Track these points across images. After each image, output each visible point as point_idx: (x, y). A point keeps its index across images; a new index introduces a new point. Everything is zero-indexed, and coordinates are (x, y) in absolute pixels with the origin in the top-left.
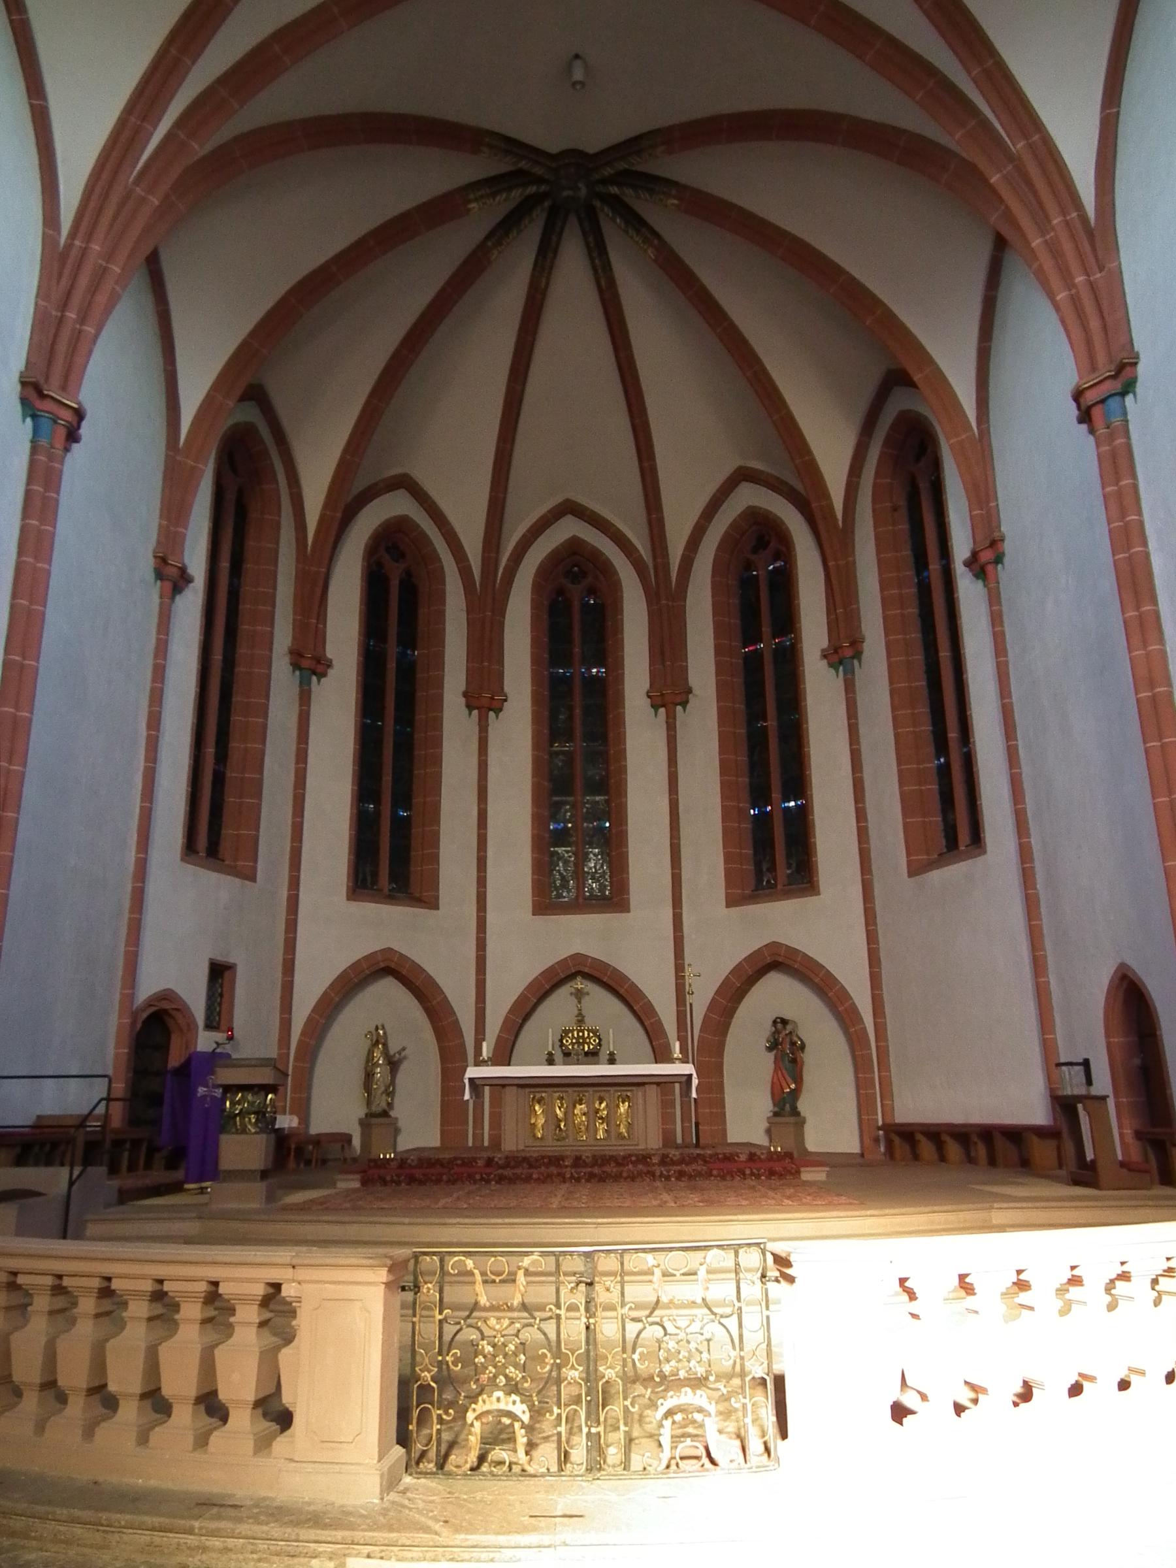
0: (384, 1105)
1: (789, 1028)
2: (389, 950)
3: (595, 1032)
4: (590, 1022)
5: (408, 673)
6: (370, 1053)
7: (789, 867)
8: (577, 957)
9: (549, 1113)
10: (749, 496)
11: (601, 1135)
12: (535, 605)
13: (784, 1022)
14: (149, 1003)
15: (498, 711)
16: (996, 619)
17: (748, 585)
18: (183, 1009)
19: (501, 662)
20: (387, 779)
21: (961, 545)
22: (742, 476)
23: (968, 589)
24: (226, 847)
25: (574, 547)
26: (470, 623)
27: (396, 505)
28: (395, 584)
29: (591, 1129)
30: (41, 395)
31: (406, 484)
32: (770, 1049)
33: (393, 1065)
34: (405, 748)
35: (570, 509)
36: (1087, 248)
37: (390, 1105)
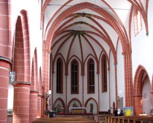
5: (60, 71)
10: (90, 57)
17: (90, 65)
21: (107, 68)
22: (90, 54)
23: (108, 71)
25: (75, 59)
27: (59, 56)
31: (60, 54)
34: (60, 79)
35: (74, 56)
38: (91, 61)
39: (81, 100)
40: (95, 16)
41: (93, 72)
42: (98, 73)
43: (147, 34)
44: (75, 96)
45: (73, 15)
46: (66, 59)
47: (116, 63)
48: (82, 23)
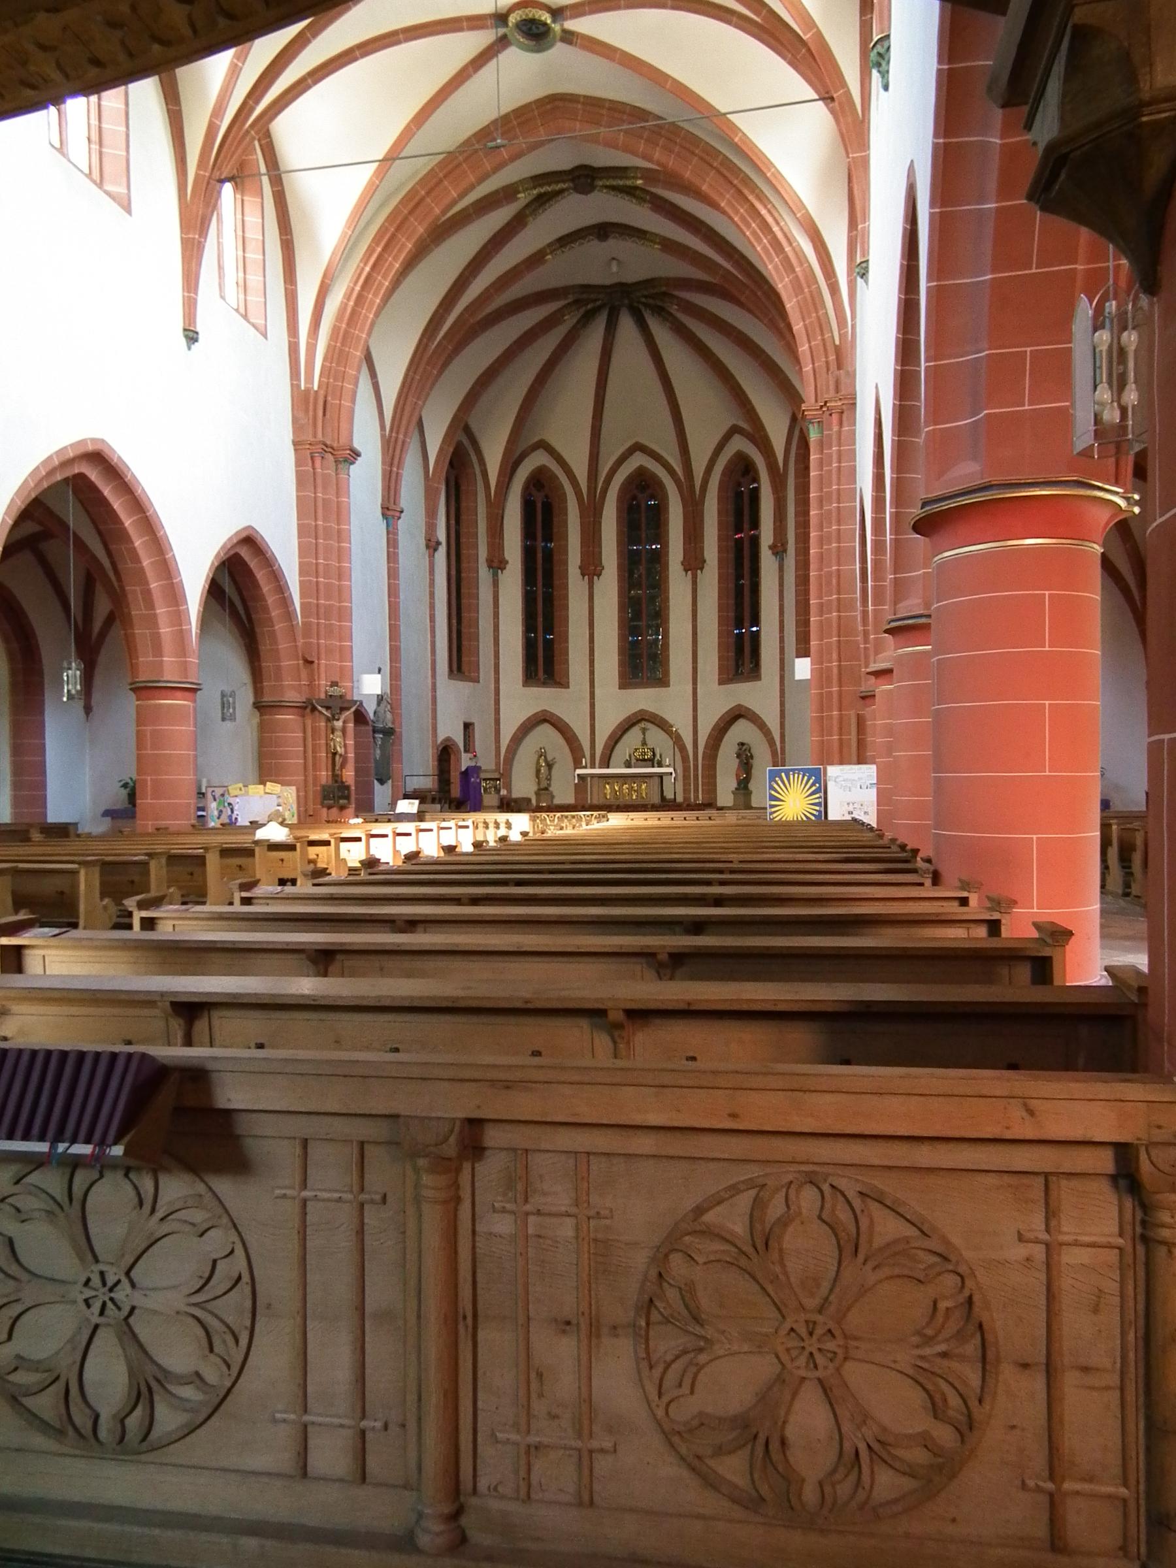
1: (744, 747)
4: (650, 744)
5: (549, 556)
6: (538, 760)
7: (751, 663)
9: (612, 788)
10: (739, 444)
11: (634, 797)
12: (619, 510)
13: (742, 744)
14: (441, 743)
15: (599, 575)
17: (739, 495)
18: (455, 744)
19: (600, 546)
20: (540, 619)
22: (734, 430)
24: (465, 667)
26: (582, 524)
28: (539, 505)
29: (630, 794)
30: (388, 509)
33: (550, 766)
34: (549, 600)
35: (638, 448)
37: (549, 785)
38: (743, 469)
41: (755, 542)
44: (643, 699)
45: (507, 194)
48: (603, 231)
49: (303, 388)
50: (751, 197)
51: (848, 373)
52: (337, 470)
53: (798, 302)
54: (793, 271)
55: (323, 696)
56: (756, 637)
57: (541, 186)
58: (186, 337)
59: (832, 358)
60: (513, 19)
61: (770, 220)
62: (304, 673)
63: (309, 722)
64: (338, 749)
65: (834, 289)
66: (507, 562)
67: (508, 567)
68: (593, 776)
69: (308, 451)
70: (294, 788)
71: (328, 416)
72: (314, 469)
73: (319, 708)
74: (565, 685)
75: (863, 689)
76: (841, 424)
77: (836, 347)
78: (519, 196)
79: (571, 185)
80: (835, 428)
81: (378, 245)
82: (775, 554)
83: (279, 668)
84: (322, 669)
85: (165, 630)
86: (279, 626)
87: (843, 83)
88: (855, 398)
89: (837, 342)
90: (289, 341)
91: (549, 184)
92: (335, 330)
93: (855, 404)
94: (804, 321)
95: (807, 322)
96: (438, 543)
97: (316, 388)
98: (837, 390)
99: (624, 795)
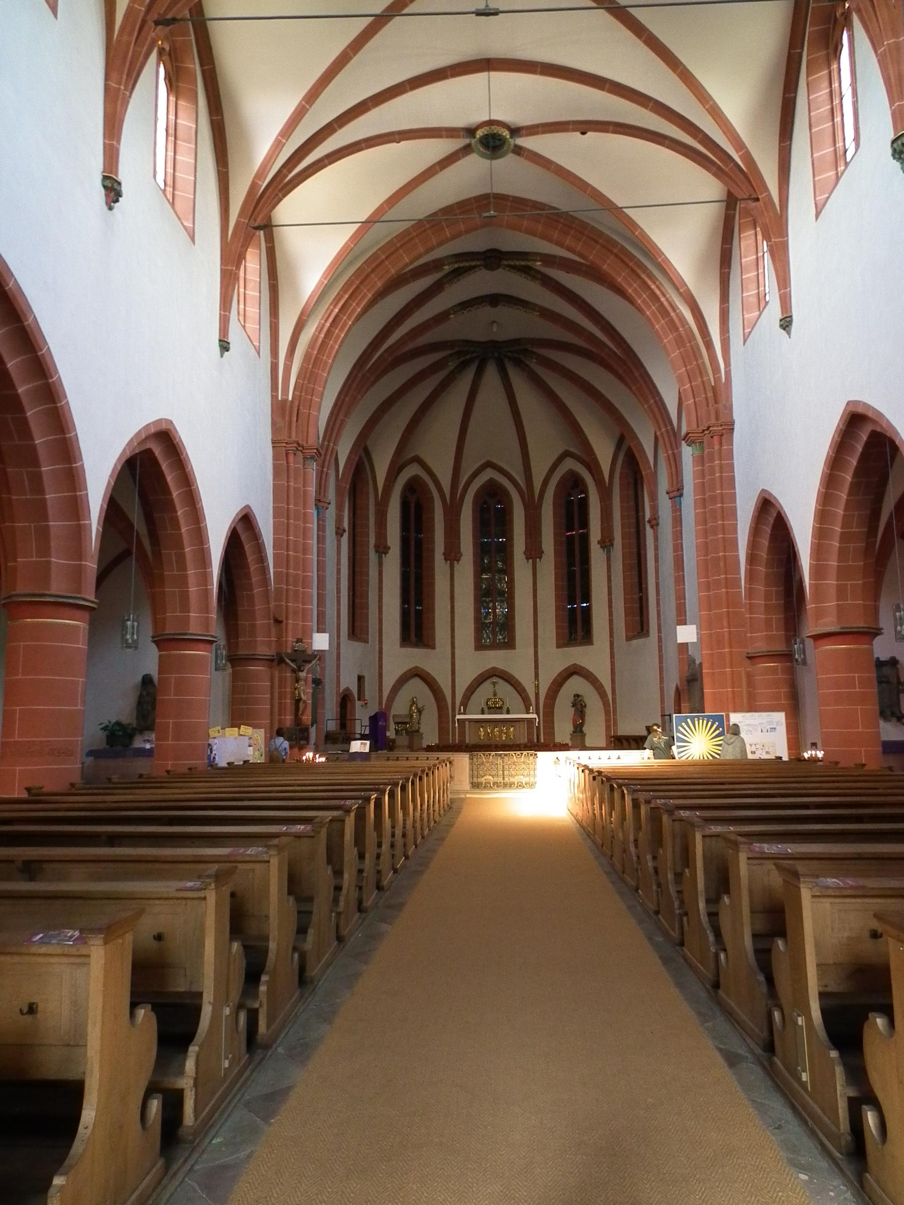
0: (417, 728)
1: (580, 698)
2: (417, 667)
3: (501, 699)
4: (499, 695)
5: (419, 544)
6: (411, 706)
7: (583, 631)
8: (493, 668)
9: (485, 731)
10: (569, 464)
11: (504, 738)
12: (474, 511)
14: (343, 692)
15: (458, 561)
16: (656, 548)
17: (569, 504)
18: (352, 694)
20: (413, 594)
21: (648, 516)
22: (566, 454)
23: (649, 531)
25: (491, 483)
26: (445, 521)
27: (413, 470)
28: (413, 505)
29: (500, 737)
30: (319, 501)
31: (418, 460)
32: (573, 706)
33: (420, 712)
34: (419, 579)
35: (489, 465)
36: (672, 438)
37: (419, 728)
38: (573, 483)
39: (526, 678)
40: (549, 260)
41: (585, 540)
42: (606, 543)
43: (786, 324)
44: (495, 659)
45: (436, 265)
46: (446, 484)
47: (676, 493)
48: (494, 300)
49: (280, 399)
50: (643, 276)
51: (725, 406)
52: (304, 465)
53: (681, 353)
54: (677, 329)
55: (289, 651)
56: (587, 612)
57: (461, 261)
58: (221, 346)
59: (710, 394)
60: (479, 133)
61: (658, 292)
62: (273, 631)
63: (277, 673)
64: (302, 696)
65: (709, 345)
66: (389, 548)
67: (390, 552)
68: (470, 720)
69: (284, 449)
70: (263, 730)
71: (300, 422)
72: (288, 463)
73: (288, 661)
74: (433, 647)
75: (750, 651)
76: (721, 444)
77: (712, 387)
78: (445, 267)
79: (483, 263)
80: (717, 447)
81: (345, 292)
82: (603, 547)
83: (253, 626)
84: (290, 627)
85: (193, 589)
86: (257, 590)
87: (766, 189)
88: (733, 425)
89: (713, 384)
90: (272, 362)
91: (467, 261)
92: (307, 357)
93: (733, 429)
94: (685, 366)
95: (688, 368)
96: (344, 531)
97: (290, 398)
98: (717, 419)
99: (495, 736)
